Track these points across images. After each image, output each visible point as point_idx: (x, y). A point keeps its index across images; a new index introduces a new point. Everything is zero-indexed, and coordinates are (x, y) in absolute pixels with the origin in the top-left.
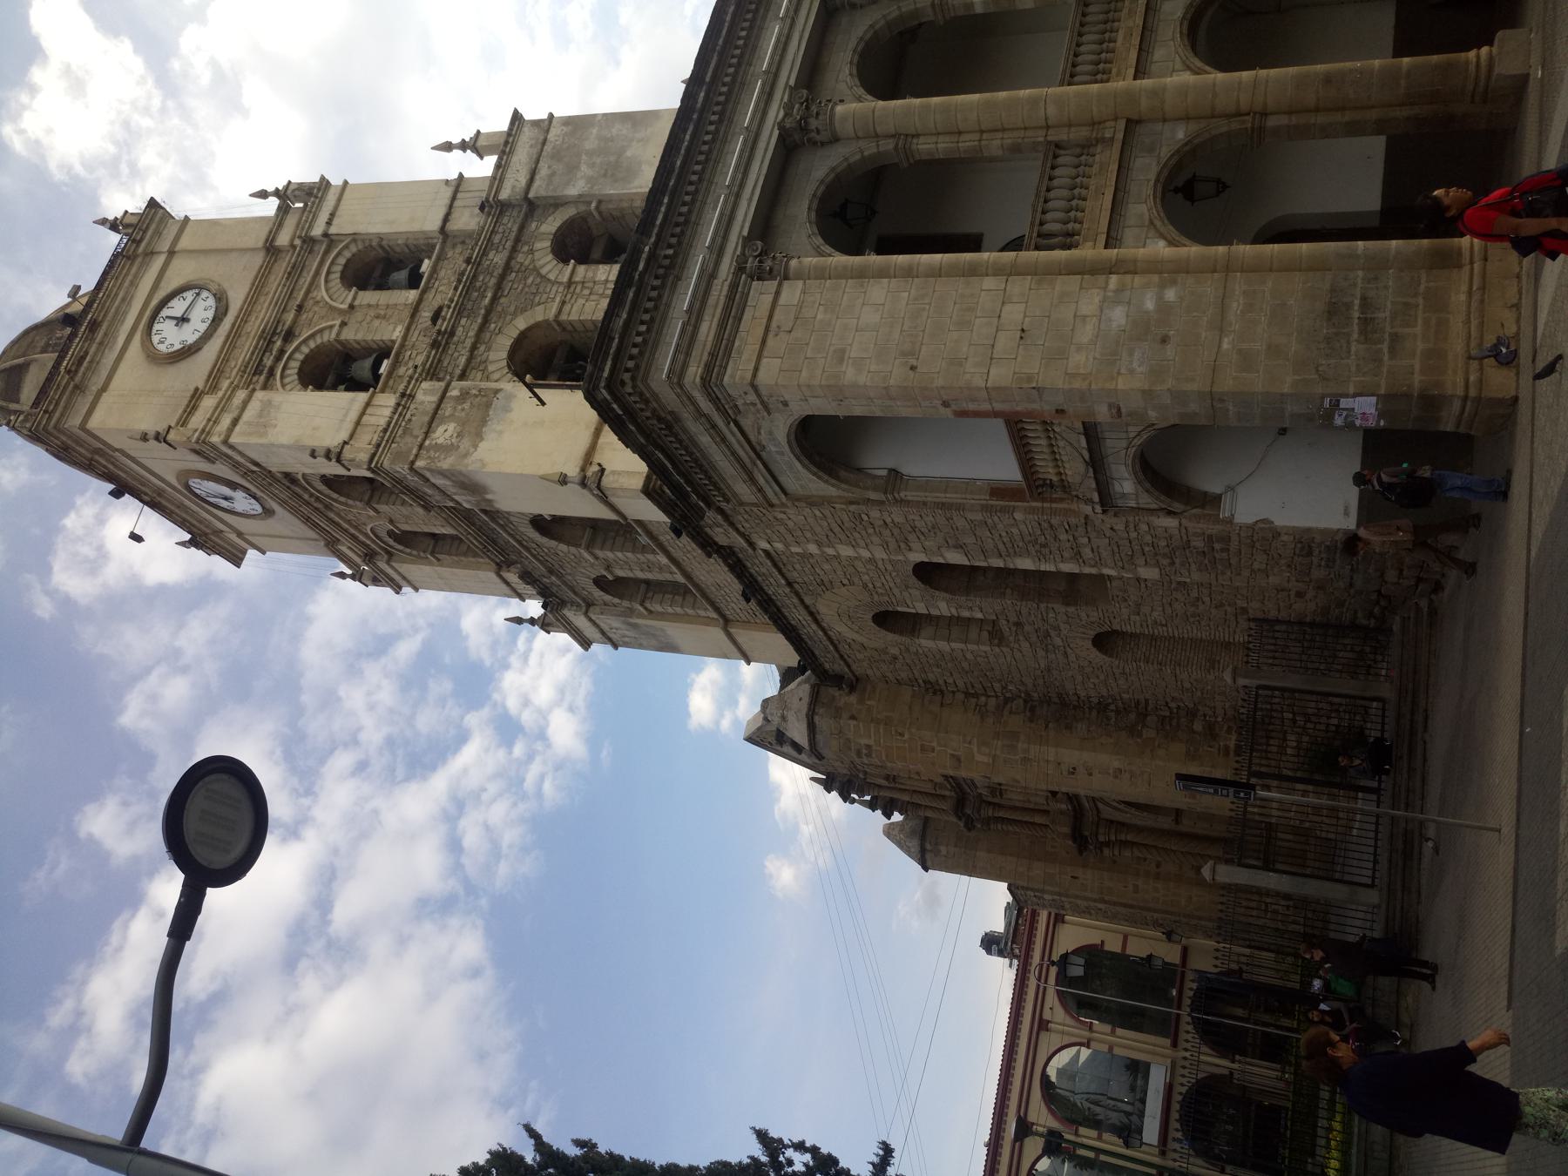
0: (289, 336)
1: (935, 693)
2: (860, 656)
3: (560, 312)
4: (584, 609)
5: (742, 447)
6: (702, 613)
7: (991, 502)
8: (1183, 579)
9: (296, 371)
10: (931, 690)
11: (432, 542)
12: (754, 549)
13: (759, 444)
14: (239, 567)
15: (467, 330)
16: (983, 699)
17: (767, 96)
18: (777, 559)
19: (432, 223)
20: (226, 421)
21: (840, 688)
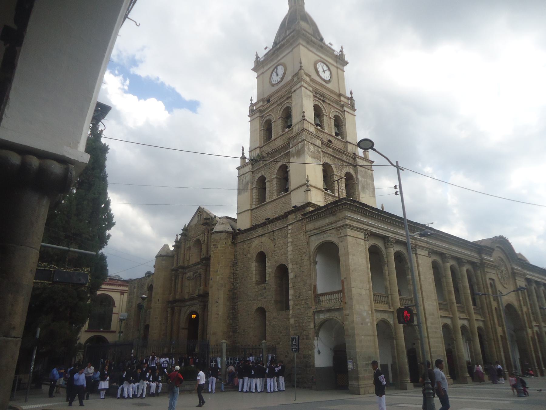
0: (323, 101)
1: (233, 265)
2: (245, 246)
3: (336, 175)
4: (252, 171)
5: (326, 229)
6: (254, 203)
7: (312, 285)
8: (291, 328)
9: (317, 104)
10: (233, 264)
11: (266, 129)
12: (288, 225)
13: (326, 233)
14: (252, 70)
15: (330, 151)
16: (233, 278)
17: (394, 233)
18: (282, 229)
19: (349, 139)
20: (306, 86)
21: (232, 240)
